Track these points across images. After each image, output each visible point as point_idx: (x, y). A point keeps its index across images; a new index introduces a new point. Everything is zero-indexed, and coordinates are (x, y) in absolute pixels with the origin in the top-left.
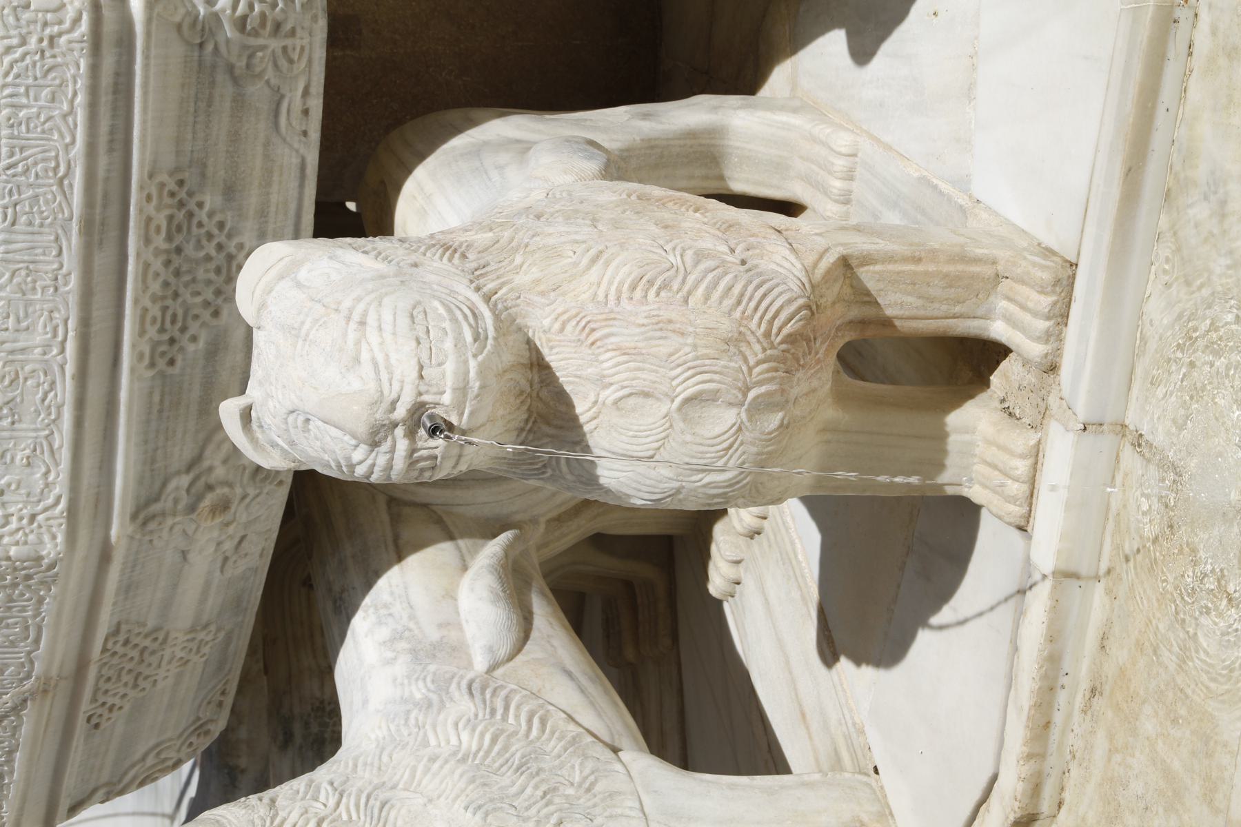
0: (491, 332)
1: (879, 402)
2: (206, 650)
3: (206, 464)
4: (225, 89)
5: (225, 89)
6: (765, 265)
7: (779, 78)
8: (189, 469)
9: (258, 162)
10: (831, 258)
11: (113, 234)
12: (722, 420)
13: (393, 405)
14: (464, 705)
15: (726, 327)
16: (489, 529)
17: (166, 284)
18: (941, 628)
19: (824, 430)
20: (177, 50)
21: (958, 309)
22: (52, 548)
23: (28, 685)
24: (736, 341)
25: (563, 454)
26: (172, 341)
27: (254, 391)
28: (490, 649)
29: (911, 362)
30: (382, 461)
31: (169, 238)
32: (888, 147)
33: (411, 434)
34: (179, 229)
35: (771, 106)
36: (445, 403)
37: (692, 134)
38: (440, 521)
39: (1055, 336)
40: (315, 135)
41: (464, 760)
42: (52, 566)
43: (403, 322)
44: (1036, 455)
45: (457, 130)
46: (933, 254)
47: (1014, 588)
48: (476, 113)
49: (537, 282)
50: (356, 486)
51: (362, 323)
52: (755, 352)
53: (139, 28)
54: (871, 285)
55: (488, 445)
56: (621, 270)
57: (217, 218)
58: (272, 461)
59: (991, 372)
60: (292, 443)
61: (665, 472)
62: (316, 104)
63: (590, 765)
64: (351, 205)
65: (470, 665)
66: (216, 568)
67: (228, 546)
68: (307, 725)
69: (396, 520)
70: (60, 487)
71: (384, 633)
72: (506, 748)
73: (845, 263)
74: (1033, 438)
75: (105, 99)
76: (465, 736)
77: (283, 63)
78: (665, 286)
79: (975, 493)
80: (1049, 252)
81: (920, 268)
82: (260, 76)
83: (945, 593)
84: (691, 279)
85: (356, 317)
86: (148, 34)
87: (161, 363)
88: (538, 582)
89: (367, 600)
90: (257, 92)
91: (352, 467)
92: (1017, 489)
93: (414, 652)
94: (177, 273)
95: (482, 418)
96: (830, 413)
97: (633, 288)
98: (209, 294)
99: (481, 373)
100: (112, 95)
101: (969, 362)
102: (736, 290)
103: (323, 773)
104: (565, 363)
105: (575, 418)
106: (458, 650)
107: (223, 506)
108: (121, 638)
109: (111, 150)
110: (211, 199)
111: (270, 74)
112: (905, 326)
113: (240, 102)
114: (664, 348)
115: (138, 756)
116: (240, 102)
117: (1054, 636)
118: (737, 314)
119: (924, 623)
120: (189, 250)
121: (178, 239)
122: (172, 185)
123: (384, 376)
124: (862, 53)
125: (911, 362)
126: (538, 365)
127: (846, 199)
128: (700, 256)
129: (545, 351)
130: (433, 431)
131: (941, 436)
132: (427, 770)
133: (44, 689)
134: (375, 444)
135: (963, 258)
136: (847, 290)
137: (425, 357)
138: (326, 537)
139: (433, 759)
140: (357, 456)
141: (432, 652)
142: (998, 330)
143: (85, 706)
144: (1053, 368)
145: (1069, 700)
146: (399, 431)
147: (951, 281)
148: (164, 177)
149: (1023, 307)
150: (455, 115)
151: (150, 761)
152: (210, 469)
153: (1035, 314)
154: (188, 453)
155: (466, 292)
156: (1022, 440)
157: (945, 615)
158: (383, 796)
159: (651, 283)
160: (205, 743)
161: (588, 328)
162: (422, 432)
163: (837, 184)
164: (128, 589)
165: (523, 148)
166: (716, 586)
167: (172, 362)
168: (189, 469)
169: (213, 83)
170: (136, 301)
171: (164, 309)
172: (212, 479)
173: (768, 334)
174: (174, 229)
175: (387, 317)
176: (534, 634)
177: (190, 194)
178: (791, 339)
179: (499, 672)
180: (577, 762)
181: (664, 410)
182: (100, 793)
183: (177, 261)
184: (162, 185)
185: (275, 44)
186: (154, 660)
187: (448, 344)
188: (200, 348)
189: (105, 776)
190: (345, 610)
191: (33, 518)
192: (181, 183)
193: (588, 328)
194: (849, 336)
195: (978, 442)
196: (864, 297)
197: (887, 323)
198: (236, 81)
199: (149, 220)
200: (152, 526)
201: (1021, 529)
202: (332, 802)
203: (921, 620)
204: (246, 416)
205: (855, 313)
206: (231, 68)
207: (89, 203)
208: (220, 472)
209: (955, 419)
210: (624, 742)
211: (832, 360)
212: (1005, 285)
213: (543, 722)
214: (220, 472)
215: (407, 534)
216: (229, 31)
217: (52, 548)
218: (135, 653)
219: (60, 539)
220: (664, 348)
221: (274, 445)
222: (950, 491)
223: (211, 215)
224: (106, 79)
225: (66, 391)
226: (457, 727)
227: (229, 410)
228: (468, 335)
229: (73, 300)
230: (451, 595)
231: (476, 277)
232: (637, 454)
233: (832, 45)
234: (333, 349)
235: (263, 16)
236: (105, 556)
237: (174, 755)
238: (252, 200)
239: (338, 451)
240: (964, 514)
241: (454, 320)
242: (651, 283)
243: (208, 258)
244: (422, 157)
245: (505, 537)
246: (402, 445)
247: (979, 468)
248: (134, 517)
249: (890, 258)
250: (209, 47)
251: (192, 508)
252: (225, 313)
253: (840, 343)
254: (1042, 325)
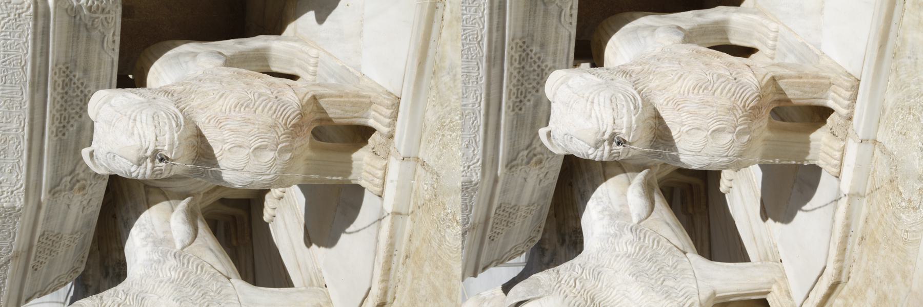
0: (183, 123)
1: (327, 149)
2: (76, 241)
3: (77, 172)
4: (84, 34)
5: (84, 34)
6: (285, 98)
7: (290, 29)
8: (70, 174)
9: (96, 60)
10: (309, 96)
11: (42, 87)
12: (268, 156)
13: (146, 150)
14: (172, 262)
15: (270, 121)
16: (182, 196)
17: (62, 105)
18: (350, 233)
19: (307, 160)
20: (66, 19)
21: (356, 115)
22: (19, 203)
23: (10, 254)
24: (274, 127)
25: (209, 168)
26: (64, 127)
27: (94, 145)
28: (182, 241)
29: (339, 134)
30: (142, 171)
31: (63, 88)
32: (330, 55)
33: (153, 161)
34: (67, 85)
35: (287, 39)
36: (165, 150)
37: (257, 50)
38: (163, 194)
39: (392, 125)
40: (117, 50)
41: (172, 282)
42: (19, 210)
43: (150, 119)
44: (385, 169)
45: (170, 48)
46: (347, 95)
47: (376, 219)
48: (177, 42)
49: (200, 105)
50: (132, 180)
51: (135, 120)
52: (281, 130)
53: (52, 10)
54: (324, 106)
55: (181, 165)
56: (231, 100)
57: (81, 81)
58: (101, 171)
59: (369, 138)
60: (109, 165)
61: (248, 175)
62: (118, 39)
63: (219, 284)
64: (130, 76)
65: (175, 247)
66: (80, 211)
67: (85, 203)
68: (114, 269)
69: (147, 193)
70: (22, 181)
71: (143, 235)
72: (188, 278)
73: (314, 98)
74: (384, 162)
75: (39, 37)
76: (173, 273)
77: (105, 23)
78: (247, 106)
79: (363, 183)
81: (342, 100)
82: (96, 28)
83: (351, 221)
84: (257, 104)
85: (132, 117)
86: (55, 13)
87: (60, 135)
88: (200, 216)
89: (137, 223)
90: (95, 34)
91: (131, 173)
92: (378, 181)
93: (154, 242)
94: (66, 101)
95: (179, 155)
96: (309, 153)
97: (235, 107)
98: (78, 109)
99: (179, 138)
100: (41, 35)
101: (361, 134)
102: (274, 108)
103: (120, 287)
104: (210, 135)
105: (214, 155)
106: (170, 241)
107: (83, 188)
108: (45, 237)
109: (41, 56)
110: (79, 74)
111: (100, 27)
112: (336, 121)
113: (89, 38)
114: (247, 129)
115: (51, 280)
116: (89, 38)
118: (274, 117)
119: (344, 231)
120: (70, 93)
121: (66, 89)
122: (64, 69)
123: (143, 140)
124: (321, 20)
125: (339, 134)
126: (200, 136)
127: (314, 74)
128: (260, 95)
129: (203, 130)
130: (161, 160)
131: (350, 162)
132: (159, 286)
133: (16, 256)
134: (139, 165)
135: (358, 96)
136: (315, 108)
137: (158, 132)
138: (121, 200)
139: (161, 282)
140: (133, 169)
141: (161, 242)
142: (371, 123)
143: (32, 262)
144: (391, 137)
146: (149, 160)
148: (61, 66)
149: (381, 114)
150: (168, 43)
151: (56, 282)
152: (78, 174)
153: (385, 117)
154: (70, 168)
155: (173, 108)
156: (380, 163)
157: (351, 228)
158: (142, 295)
159: (242, 105)
160: (76, 276)
162: (157, 160)
163: (311, 69)
164: (48, 219)
165: (195, 55)
166: (266, 218)
167: (64, 134)
168: (70, 174)
169: (79, 31)
170: (51, 112)
171: (61, 115)
172: (79, 178)
173: (285, 124)
174: (65, 85)
175: (144, 117)
176: (199, 235)
177: (71, 72)
178: (294, 126)
179: (185, 250)
180: (214, 283)
181: (247, 152)
182: (37, 295)
183: (66, 97)
184: (60, 69)
185: (102, 16)
186: (57, 245)
187: (167, 128)
188: (74, 129)
189: (39, 289)
190: (128, 226)
191: (12, 192)
192: (67, 68)
194: (316, 125)
195: (364, 164)
196: (321, 110)
197: (330, 120)
198: (88, 30)
199: (55, 82)
200: (57, 195)
201: (380, 196)
202: (123, 298)
203: (343, 230)
204: (92, 154)
205: (318, 116)
206: (86, 25)
207: (33, 75)
208: (82, 175)
209: (355, 155)
210: (232, 275)
211: (310, 133)
212: (374, 106)
213: (202, 268)
214: (82, 175)
215: (151, 198)
216: (85, 11)
217: (19, 203)
218: (50, 243)
219: (22, 200)
220: (247, 129)
221: (102, 165)
222: (353, 182)
223: (78, 80)
224: (40, 29)
225: (25, 145)
226: (170, 270)
227: (85, 152)
228: (174, 125)
229: (27, 111)
230: (168, 221)
231: (177, 103)
232: (237, 169)
233: (310, 17)
234: (124, 130)
235: (98, 6)
236: (39, 206)
237: (64, 280)
238: (94, 74)
239: (126, 167)
240: (359, 191)
241: (169, 119)
242: (242, 105)
243: (77, 96)
244: (157, 58)
245: (188, 199)
246: (150, 165)
247: (364, 174)
248: (50, 192)
249: (331, 96)
250: (78, 18)
251: (71, 189)
252: (84, 116)
253: (313, 127)
254: (388, 121)
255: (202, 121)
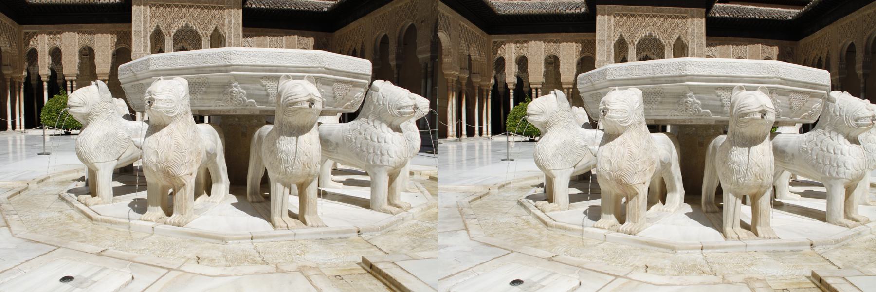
4: (221, 90)
6: (182, 168)
15: (170, 159)
20: (226, 81)
80: (186, 223)
90: (222, 96)
96: (160, 185)
100: (218, 69)
113: (220, 93)
116: (220, 93)
117: (119, 223)
131: (157, 206)
145: (108, 225)
147: (182, 206)
161: (170, 134)
193: (170, 134)
209: (160, 208)
255: (172, 127)
